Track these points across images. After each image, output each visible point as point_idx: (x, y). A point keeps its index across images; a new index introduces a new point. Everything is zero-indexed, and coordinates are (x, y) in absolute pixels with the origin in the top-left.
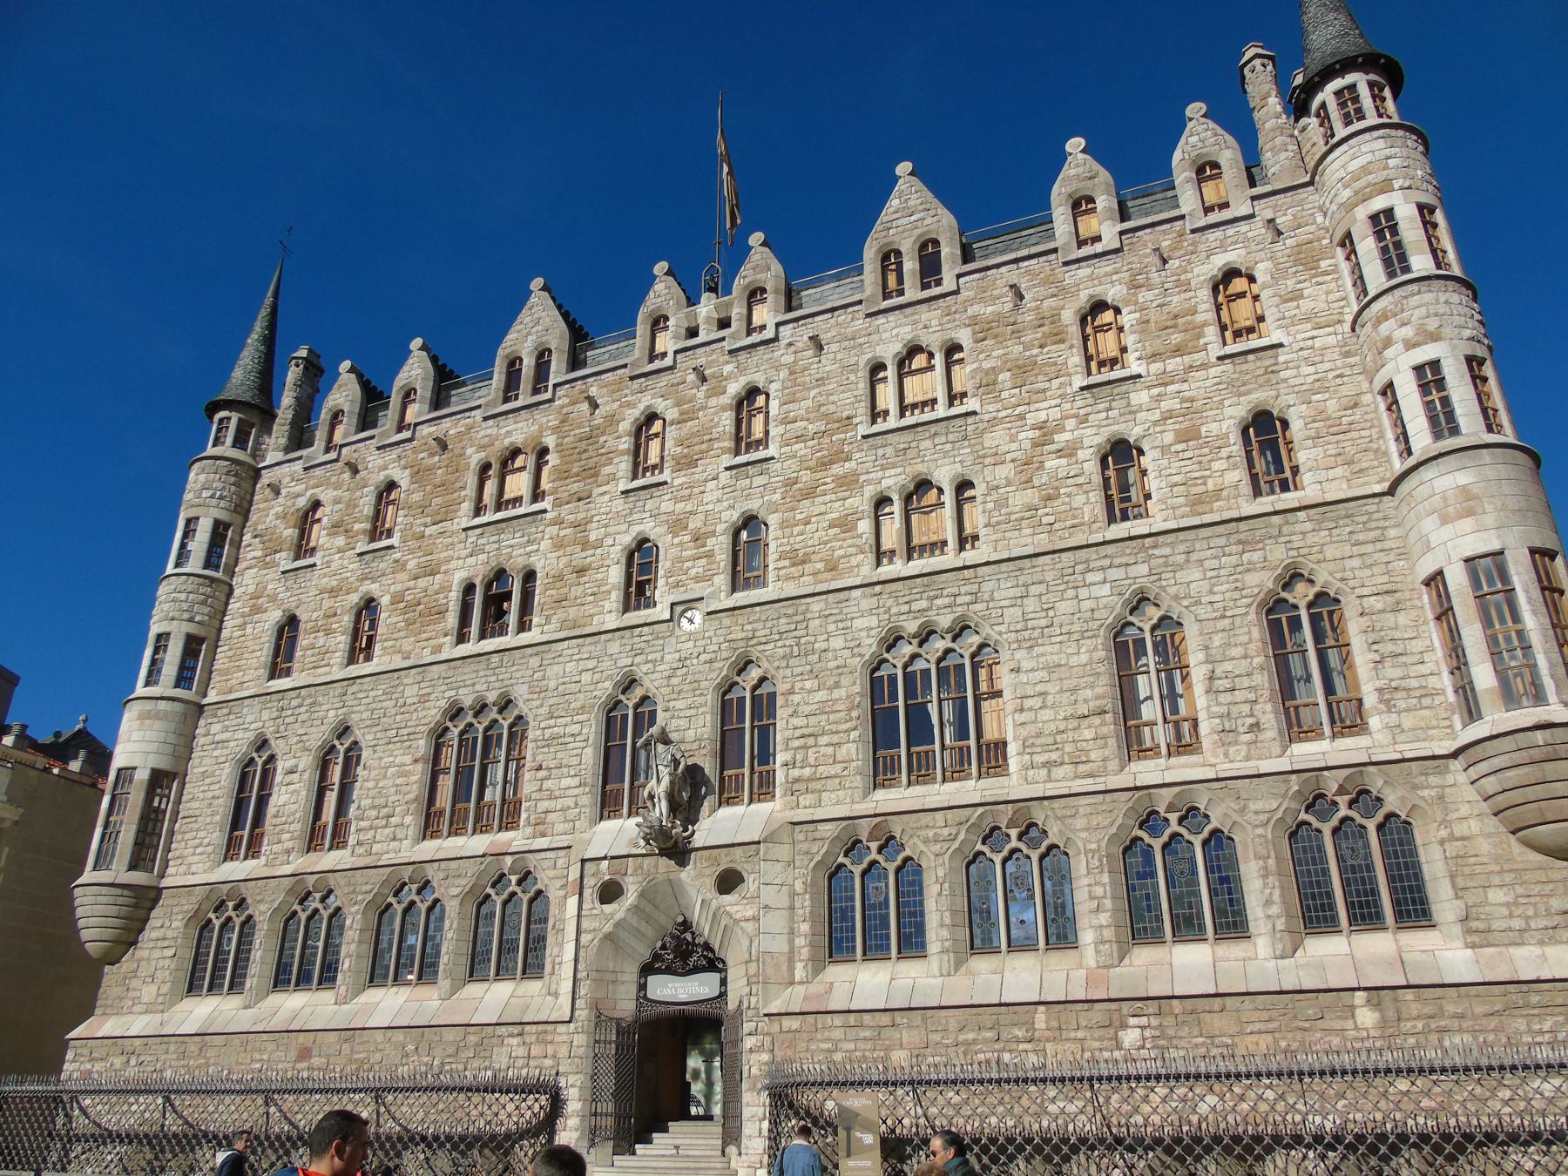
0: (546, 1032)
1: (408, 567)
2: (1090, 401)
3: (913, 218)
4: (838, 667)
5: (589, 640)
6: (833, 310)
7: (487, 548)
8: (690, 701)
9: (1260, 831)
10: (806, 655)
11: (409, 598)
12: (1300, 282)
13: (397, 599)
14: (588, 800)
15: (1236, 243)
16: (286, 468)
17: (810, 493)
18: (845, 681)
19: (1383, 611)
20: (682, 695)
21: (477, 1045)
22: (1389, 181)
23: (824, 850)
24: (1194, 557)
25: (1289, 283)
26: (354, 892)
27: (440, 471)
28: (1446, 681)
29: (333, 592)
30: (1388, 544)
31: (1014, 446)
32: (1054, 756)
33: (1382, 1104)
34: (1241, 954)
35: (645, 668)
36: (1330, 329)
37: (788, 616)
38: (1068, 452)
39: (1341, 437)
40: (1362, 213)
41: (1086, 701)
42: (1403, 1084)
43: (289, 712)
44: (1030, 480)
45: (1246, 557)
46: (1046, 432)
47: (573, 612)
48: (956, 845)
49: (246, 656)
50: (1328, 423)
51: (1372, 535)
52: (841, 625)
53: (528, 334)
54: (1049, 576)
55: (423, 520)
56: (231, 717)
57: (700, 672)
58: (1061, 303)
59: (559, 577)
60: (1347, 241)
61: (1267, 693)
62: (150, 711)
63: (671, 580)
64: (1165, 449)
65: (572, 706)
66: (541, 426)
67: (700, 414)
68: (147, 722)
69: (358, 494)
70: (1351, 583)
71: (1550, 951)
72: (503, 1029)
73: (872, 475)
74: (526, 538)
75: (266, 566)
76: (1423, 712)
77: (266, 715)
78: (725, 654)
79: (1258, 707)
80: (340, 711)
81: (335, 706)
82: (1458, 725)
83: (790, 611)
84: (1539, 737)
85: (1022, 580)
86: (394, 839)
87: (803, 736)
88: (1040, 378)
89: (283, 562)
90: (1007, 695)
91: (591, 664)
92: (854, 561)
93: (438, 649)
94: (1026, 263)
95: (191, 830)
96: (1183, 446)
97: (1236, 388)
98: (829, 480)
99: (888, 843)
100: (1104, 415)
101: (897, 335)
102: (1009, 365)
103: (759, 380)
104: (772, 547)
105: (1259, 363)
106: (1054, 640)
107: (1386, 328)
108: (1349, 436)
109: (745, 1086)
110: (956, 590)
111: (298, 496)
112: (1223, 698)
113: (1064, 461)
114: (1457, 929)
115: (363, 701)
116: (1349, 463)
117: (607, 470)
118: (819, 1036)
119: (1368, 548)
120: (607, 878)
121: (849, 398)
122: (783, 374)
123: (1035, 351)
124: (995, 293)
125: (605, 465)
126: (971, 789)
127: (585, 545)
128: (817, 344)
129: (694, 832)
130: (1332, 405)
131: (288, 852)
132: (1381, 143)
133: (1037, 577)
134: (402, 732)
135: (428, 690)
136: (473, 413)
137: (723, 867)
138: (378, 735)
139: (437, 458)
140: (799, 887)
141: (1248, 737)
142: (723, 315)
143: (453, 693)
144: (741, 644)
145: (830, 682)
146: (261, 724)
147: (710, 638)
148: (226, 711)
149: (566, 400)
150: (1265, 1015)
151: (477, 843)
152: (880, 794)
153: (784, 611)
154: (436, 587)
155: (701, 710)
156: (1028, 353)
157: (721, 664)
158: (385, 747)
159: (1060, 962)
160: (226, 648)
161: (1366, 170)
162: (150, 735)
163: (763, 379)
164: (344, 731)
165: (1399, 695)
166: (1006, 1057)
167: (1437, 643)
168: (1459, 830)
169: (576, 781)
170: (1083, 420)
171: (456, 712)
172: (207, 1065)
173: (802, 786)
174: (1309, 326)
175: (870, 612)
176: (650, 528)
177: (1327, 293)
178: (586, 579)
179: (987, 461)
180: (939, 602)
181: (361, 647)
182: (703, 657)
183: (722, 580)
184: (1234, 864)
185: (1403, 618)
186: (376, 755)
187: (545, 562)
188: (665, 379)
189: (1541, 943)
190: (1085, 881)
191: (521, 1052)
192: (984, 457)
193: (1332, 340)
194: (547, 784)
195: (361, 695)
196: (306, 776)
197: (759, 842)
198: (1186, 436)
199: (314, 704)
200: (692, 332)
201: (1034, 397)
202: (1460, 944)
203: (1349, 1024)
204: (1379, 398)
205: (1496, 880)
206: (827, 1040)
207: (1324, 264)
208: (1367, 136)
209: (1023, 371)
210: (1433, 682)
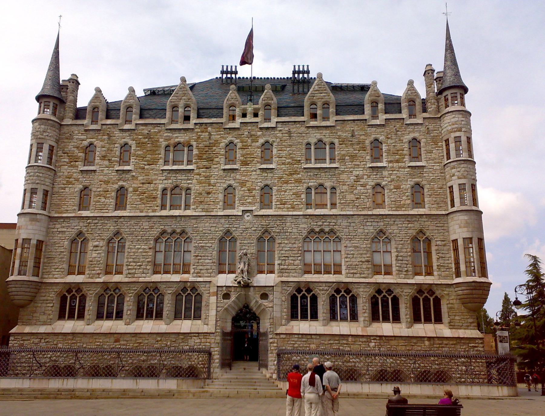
0: (206, 336)
1: (139, 179)
2: (372, 171)
3: (322, 95)
4: (295, 238)
5: (213, 217)
6: (295, 122)
7: (172, 178)
8: (249, 241)
9: (406, 297)
10: (285, 233)
11: (140, 190)
12: (432, 148)
13: (135, 190)
14: (215, 268)
15: (417, 131)
16: (75, 128)
17: (287, 182)
18: (297, 242)
19: (440, 246)
21: (183, 339)
22: (461, 128)
23: (291, 290)
24: (396, 223)
25: (430, 147)
26: (129, 289)
27: (149, 145)
28: (453, 265)
29: (107, 182)
30: (445, 228)
31: (349, 180)
32: (355, 271)
33: (428, 363)
34: (399, 327)
35: (234, 229)
36: (438, 164)
37: (280, 220)
39: (437, 196)
40: (453, 135)
41: (364, 258)
42: (432, 359)
43: (93, 225)
44: (353, 192)
45: (409, 225)
47: (206, 207)
48: (328, 292)
49: (66, 200)
50: (434, 191)
51: (441, 225)
52: (296, 225)
53: (181, 99)
54: (357, 221)
55: (143, 162)
56: (64, 223)
58: (366, 138)
60: (447, 141)
61: (410, 262)
62: (34, 218)
63: (241, 202)
64: (391, 190)
65: (208, 237)
66: (190, 138)
67: (250, 147)
68: (33, 222)
69: (112, 146)
70: (434, 237)
71: (467, 331)
72: (192, 334)
73: (306, 181)
74: (187, 178)
75: (72, 166)
76: (447, 272)
77: (81, 224)
78: (260, 229)
79: (408, 265)
80: (115, 227)
81: (113, 225)
82: (454, 276)
83: (281, 219)
84: (473, 284)
85: (349, 221)
86: (143, 273)
87: (284, 257)
88: (358, 160)
89: (79, 166)
90: (343, 253)
91: (215, 225)
92: (300, 206)
93: (154, 211)
94: (357, 122)
95: (52, 263)
96: (396, 190)
97: (412, 176)
98: (293, 179)
99: (309, 290)
100: (375, 176)
101: (315, 136)
102: (349, 155)
103: (271, 140)
104: (274, 197)
105: (419, 170)
106: (357, 239)
107: (453, 170)
108: (439, 196)
109: (269, 352)
110: (330, 221)
111: (83, 140)
112: (399, 262)
113: (363, 188)
114: (448, 325)
115: (125, 225)
116: (438, 204)
117: (216, 159)
118: (291, 339)
119: (439, 228)
120: (225, 292)
121: (300, 154)
122: (278, 140)
123: (357, 152)
124: (346, 129)
125: (216, 158)
127: (210, 185)
128: (289, 132)
129: (253, 280)
131: (99, 274)
132: (461, 116)
133: (353, 221)
134: (143, 238)
135: (152, 225)
136: (161, 126)
138: (134, 237)
139: (147, 140)
140: (283, 299)
141: (405, 273)
142: (256, 112)
143: (163, 227)
144: (266, 226)
145: (293, 242)
146: (79, 227)
147: (255, 223)
148: (62, 220)
149: (199, 130)
150: (404, 341)
151: (176, 278)
152: (306, 276)
153: (279, 218)
154: (152, 189)
156: (355, 152)
158: (136, 242)
159: (354, 324)
160: (57, 196)
161: (455, 123)
162: (35, 227)
163: (271, 140)
164: (117, 233)
165: (442, 267)
166: (340, 347)
167: (452, 256)
168: (451, 302)
169: (211, 261)
170: (369, 177)
171: (163, 232)
173: (284, 271)
174: (433, 162)
175: (305, 223)
176: (232, 182)
177: (439, 153)
178: (210, 196)
179: (341, 183)
180: (325, 223)
181: (120, 204)
182: (253, 229)
183: (258, 205)
184: (398, 304)
185: (445, 248)
186: (133, 244)
187: (195, 187)
189: (465, 329)
190: (362, 305)
191: (199, 341)
192: (340, 182)
193: (438, 168)
194: (200, 261)
195: (125, 223)
197: (273, 286)
198: (397, 187)
200: (244, 115)
201: (356, 166)
202: (448, 328)
203: (423, 344)
204: (448, 188)
205: (457, 314)
206: (293, 341)
207: (440, 144)
208: (458, 113)
209: (353, 157)
210: (450, 265)
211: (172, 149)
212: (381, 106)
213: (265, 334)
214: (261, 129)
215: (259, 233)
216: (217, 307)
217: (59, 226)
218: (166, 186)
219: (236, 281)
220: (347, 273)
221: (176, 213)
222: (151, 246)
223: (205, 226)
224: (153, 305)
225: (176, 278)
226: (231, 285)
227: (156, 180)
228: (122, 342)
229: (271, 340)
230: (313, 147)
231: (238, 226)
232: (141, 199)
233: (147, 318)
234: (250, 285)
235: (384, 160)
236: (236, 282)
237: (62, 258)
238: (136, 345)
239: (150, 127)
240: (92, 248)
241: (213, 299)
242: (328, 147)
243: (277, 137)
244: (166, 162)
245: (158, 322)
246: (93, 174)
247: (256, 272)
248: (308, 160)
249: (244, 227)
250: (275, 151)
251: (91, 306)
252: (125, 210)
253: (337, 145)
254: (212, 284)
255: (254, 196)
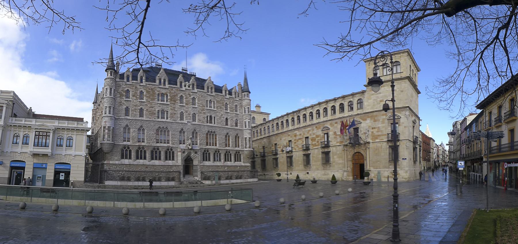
13: (147, 110)
17: (201, 113)
21: (170, 167)
27: (151, 93)
29: (136, 106)
38: (223, 117)
46: (222, 115)
47: (174, 119)
59: (172, 114)
69: (137, 91)
77: (127, 122)
93: (155, 119)
97: (236, 116)
104: (197, 118)
117: (177, 101)
121: (205, 104)
122: (198, 97)
126: (214, 147)
127: (175, 111)
130: (241, 121)
131: (136, 142)
139: (150, 90)
151: (166, 145)
164: (141, 126)
171: (160, 127)
172: (131, 168)
175: (206, 128)
176: (183, 111)
181: (141, 115)
188: (184, 92)
191: (175, 168)
194: (174, 139)
196: (137, 132)
198: (232, 120)
199: (136, 122)
200: (185, 86)
211: (160, 95)
212: (227, 92)
213: (196, 166)
214: (192, 92)
216: (181, 156)
217: (119, 122)
218: (159, 109)
220: (219, 146)
221: (164, 120)
222: (155, 132)
223: (174, 126)
224: (157, 155)
225: (166, 145)
227: (155, 106)
228: (149, 168)
229: (199, 168)
230: (208, 102)
232: (150, 114)
233: (155, 160)
235: (229, 110)
237: (121, 135)
238: (154, 169)
239: (151, 86)
240: (132, 132)
241: (179, 154)
242: (213, 103)
243: (197, 96)
244: (158, 100)
245: (160, 161)
246: (130, 102)
248: (207, 106)
250: (196, 101)
251: (133, 154)
252: (143, 117)
253: (215, 102)
254: (178, 148)
255: (190, 117)
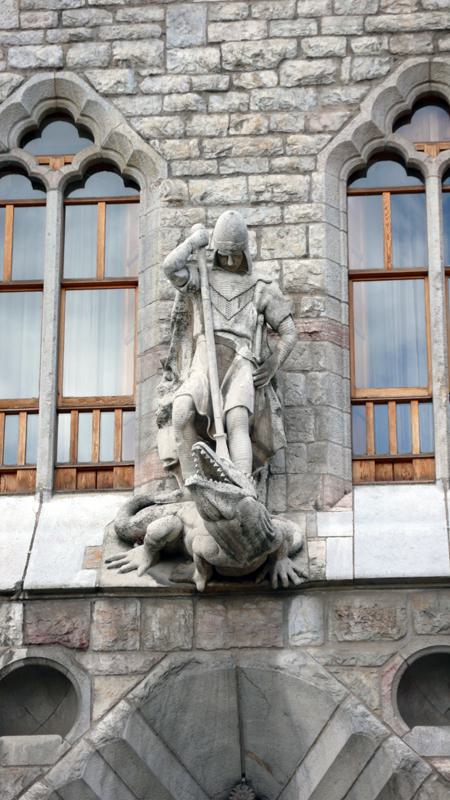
8: (257, 182)
20: (231, 165)
35: (106, 79)
57: (285, 108)
78: (365, 67)
120: (21, 653)
137: (416, 646)
155: (294, 211)
157: (355, 92)
182: (296, 69)
215: (354, 107)
219: (128, 540)
226: (84, 579)
231: (150, 50)
234: (286, 567)
236: (138, 555)
247: (337, 463)
249: (212, 56)
